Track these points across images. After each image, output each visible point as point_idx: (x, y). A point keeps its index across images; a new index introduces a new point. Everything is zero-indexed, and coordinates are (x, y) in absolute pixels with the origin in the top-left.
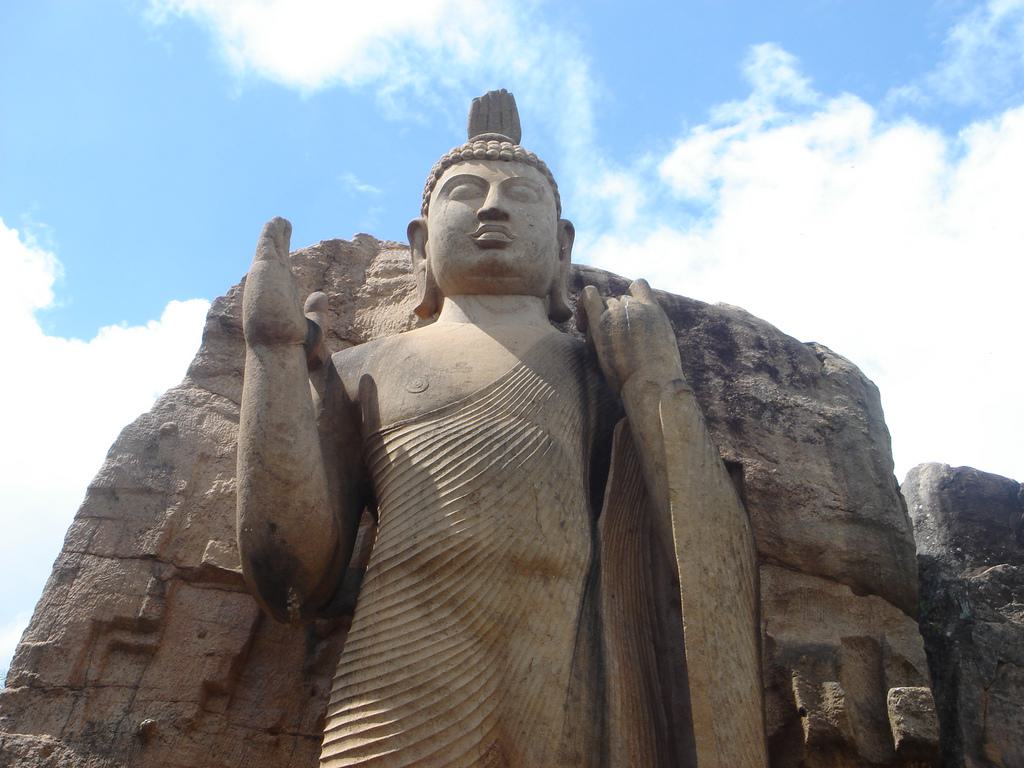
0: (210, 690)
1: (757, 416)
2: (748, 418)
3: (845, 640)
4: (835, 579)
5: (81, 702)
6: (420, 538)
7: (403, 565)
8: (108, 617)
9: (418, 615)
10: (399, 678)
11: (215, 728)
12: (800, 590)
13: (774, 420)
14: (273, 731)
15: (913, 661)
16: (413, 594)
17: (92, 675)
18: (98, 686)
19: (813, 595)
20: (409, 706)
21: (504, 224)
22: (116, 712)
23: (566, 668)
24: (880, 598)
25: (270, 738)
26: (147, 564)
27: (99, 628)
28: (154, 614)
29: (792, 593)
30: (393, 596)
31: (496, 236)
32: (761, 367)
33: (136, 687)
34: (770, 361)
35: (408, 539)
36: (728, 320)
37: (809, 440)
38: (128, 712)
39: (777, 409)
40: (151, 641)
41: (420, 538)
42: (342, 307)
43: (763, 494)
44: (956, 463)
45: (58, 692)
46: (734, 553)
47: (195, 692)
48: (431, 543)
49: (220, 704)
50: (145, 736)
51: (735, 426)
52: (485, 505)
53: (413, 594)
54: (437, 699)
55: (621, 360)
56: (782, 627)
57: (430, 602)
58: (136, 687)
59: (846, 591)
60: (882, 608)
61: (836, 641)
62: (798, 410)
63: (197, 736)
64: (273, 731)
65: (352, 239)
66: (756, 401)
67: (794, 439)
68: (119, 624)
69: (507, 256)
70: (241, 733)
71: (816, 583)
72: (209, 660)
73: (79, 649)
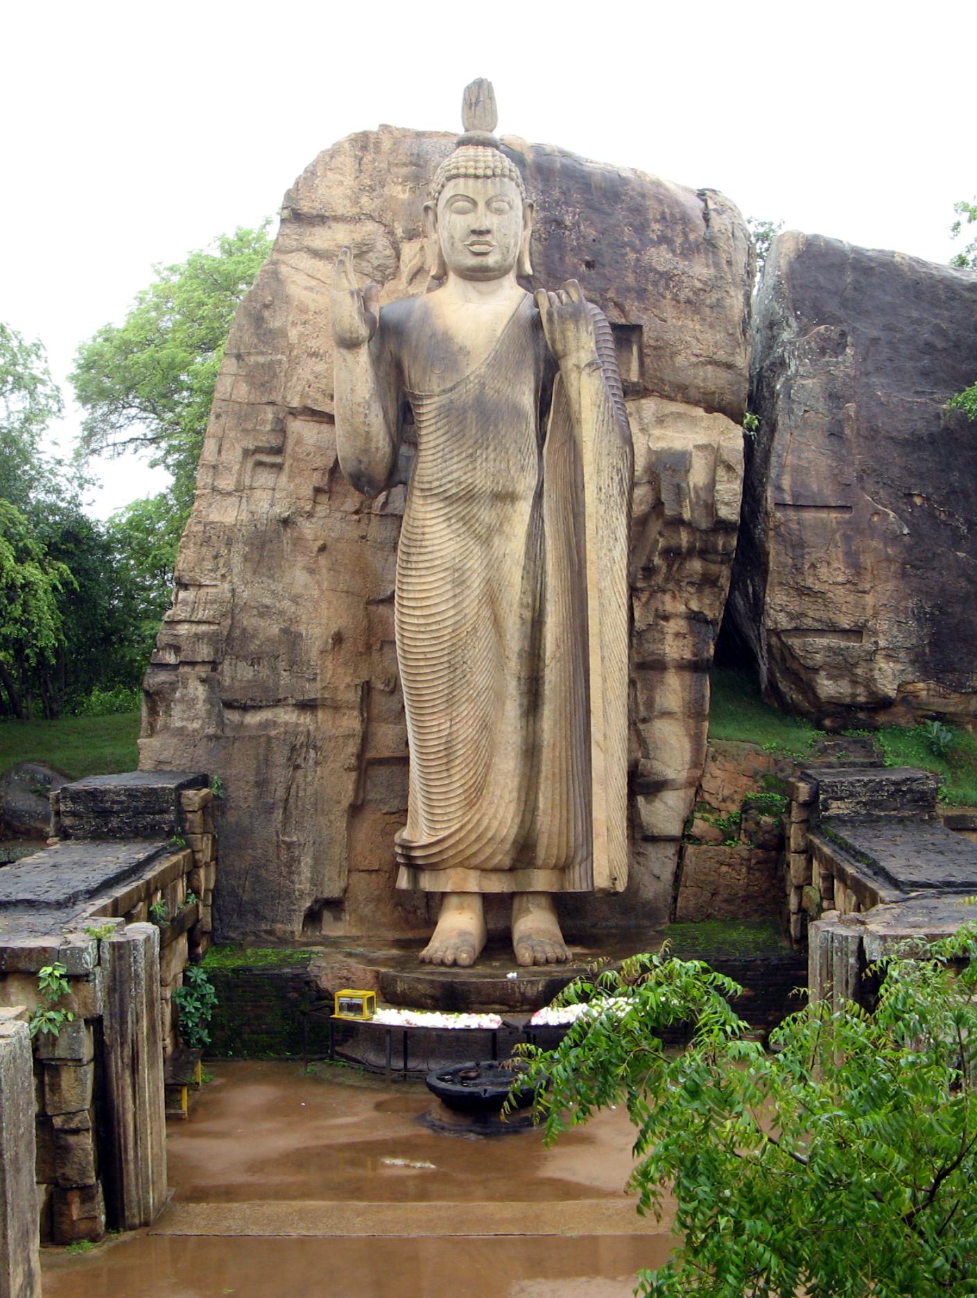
0: (318, 490)
1: (655, 284)
2: (650, 288)
3: (695, 447)
4: (696, 404)
5: (244, 500)
6: (444, 481)
8: (251, 447)
9: (444, 525)
11: (323, 514)
12: (672, 413)
13: (667, 287)
14: (356, 512)
15: (733, 462)
16: (441, 513)
17: (247, 482)
18: (251, 488)
19: (679, 416)
20: (442, 579)
21: (488, 238)
22: (265, 505)
23: (522, 557)
24: (721, 415)
25: (356, 517)
27: (246, 453)
29: (666, 415)
33: (274, 489)
34: (669, 233)
35: (437, 480)
36: (643, 196)
37: (689, 302)
39: (668, 277)
40: (278, 460)
41: (444, 481)
42: (374, 194)
43: (655, 348)
44: (809, 230)
45: (229, 494)
46: (619, 471)
48: (449, 486)
49: (323, 498)
51: (641, 294)
52: (479, 461)
53: (441, 513)
54: (457, 575)
56: (658, 438)
57: (449, 519)
58: (274, 489)
59: (700, 412)
60: (722, 420)
61: (690, 447)
62: (683, 278)
63: (314, 520)
64: (356, 512)
65: (375, 128)
66: (657, 272)
67: (678, 302)
68: (258, 450)
69: (491, 260)
70: (339, 515)
71: (680, 407)
73: (237, 467)
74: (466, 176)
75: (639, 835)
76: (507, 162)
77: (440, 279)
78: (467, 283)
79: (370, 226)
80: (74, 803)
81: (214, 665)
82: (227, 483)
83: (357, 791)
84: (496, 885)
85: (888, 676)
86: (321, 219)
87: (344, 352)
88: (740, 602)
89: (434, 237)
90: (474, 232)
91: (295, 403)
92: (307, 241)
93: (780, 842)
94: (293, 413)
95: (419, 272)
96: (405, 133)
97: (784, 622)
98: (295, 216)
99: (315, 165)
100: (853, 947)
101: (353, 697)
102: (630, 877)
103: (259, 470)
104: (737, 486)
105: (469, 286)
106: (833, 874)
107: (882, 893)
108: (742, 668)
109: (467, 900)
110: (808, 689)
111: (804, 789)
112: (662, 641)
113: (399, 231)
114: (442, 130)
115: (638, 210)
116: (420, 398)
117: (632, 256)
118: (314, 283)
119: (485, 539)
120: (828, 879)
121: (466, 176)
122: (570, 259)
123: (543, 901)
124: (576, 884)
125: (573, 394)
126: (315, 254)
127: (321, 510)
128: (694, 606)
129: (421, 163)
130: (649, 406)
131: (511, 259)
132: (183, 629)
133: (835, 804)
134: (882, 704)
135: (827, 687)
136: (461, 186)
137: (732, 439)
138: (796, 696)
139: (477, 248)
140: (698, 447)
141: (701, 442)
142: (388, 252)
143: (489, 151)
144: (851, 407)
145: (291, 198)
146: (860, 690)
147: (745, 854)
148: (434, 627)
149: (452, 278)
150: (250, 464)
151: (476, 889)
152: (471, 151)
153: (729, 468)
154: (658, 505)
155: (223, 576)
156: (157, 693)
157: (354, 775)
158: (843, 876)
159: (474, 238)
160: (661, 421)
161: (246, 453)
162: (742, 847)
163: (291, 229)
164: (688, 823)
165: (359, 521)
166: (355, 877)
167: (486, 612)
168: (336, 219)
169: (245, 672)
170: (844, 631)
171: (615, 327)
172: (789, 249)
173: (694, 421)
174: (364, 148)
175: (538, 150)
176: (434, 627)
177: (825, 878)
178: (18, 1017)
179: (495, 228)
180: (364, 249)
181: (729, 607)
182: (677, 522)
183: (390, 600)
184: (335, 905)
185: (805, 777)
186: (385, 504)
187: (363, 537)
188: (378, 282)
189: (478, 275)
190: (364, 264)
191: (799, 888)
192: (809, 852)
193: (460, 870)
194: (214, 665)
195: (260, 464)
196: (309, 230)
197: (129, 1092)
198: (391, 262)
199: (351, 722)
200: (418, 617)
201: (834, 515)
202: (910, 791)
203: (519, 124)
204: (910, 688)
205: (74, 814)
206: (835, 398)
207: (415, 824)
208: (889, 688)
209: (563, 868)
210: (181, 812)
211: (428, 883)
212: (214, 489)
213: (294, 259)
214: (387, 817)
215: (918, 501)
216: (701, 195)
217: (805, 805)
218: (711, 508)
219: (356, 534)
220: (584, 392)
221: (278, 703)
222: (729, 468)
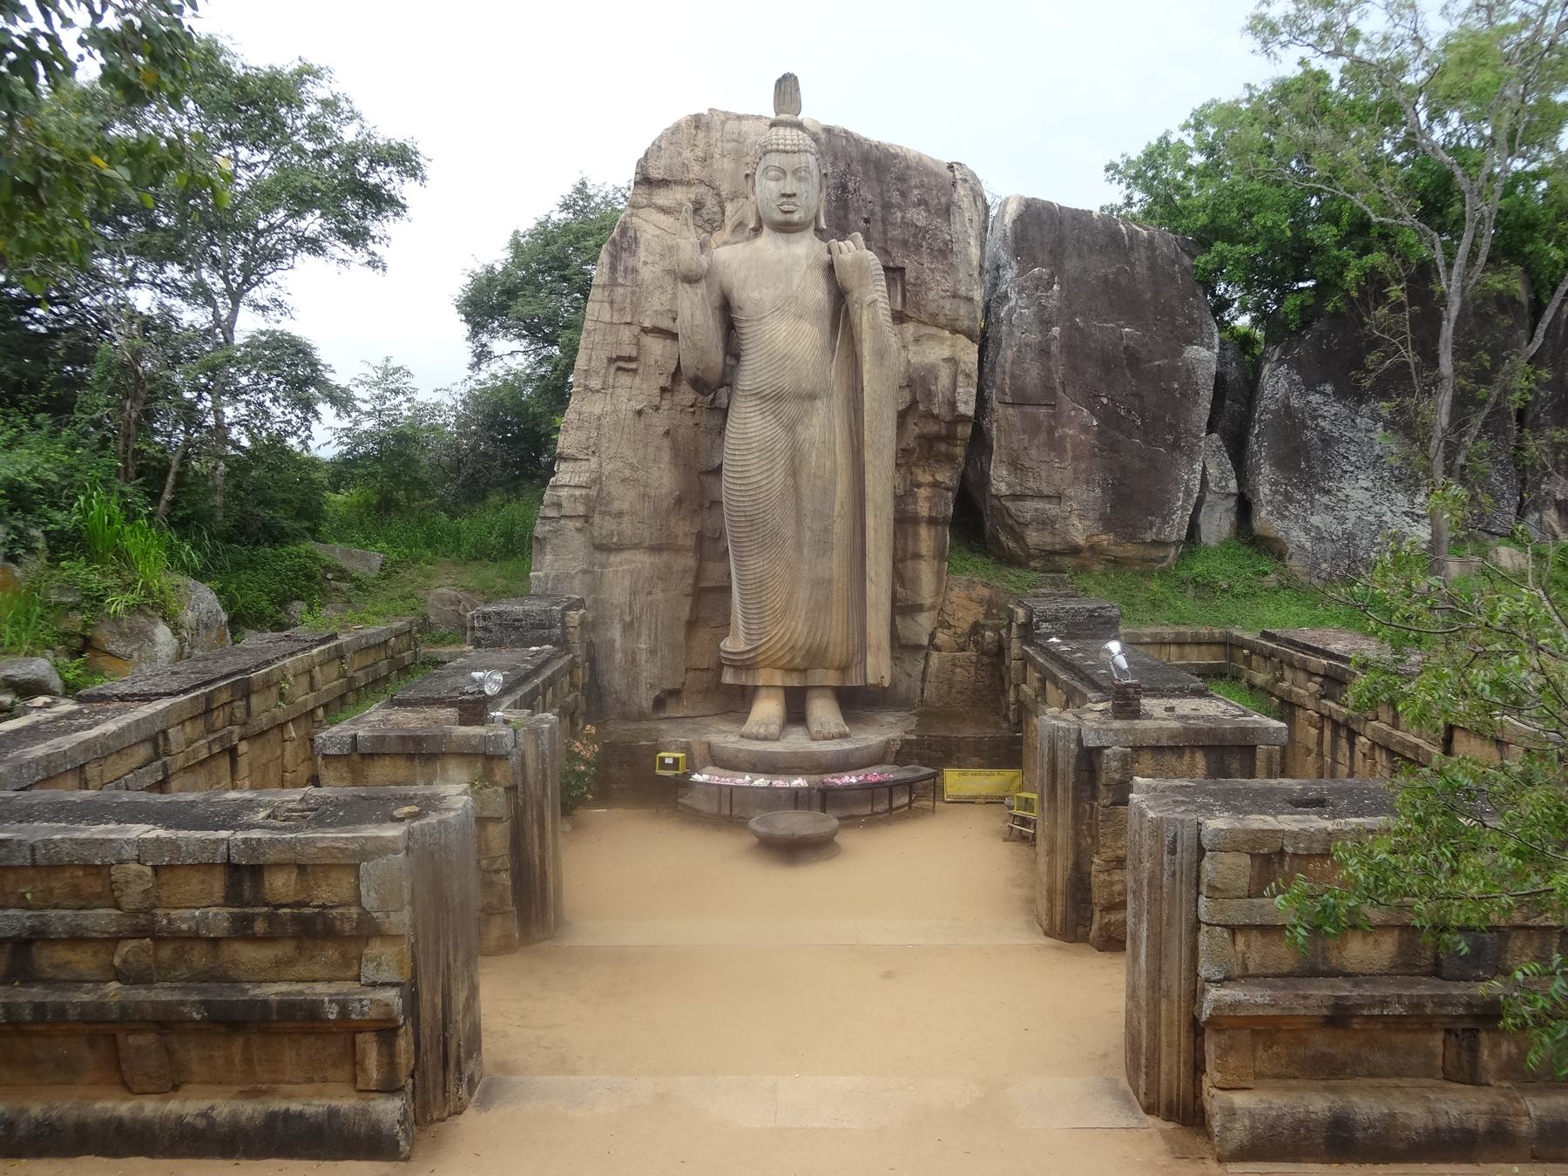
0: (663, 390)
19: (931, 337)
27: (611, 360)
28: (634, 354)
31: (791, 208)
32: (920, 203)
36: (908, 167)
40: (633, 366)
44: (1029, 195)
47: (657, 392)
49: (667, 395)
50: (640, 413)
60: (962, 340)
65: (706, 112)
68: (620, 358)
69: (795, 217)
71: (934, 330)
75: (900, 646)
76: (809, 141)
77: (757, 231)
79: (702, 189)
81: (586, 518)
82: (595, 383)
83: (692, 610)
84: (794, 681)
85: (1078, 532)
86: (664, 183)
87: (687, 286)
88: (971, 475)
89: (752, 198)
90: (784, 195)
91: (647, 324)
93: (1000, 650)
94: (645, 331)
95: (740, 225)
96: (728, 117)
97: (1003, 488)
98: (645, 181)
99: (660, 138)
100: (1074, 736)
101: (690, 542)
102: (892, 675)
104: (974, 391)
105: (780, 239)
106: (1046, 677)
107: (1090, 695)
108: (974, 524)
109: (772, 691)
110: (1020, 538)
111: (1021, 614)
112: (916, 502)
113: (724, 194)
115: (902, 179)
117: (899, 215)
118: (659, 232)
119: (791, 428)
120: (1043, 681)
122: (852, 217)
123: (829, 693)
124: (855, 680)
125: (857, 320)
126: (663, 210)
127: (666, 405)
128: (939, 477)
130: (910, 329)
131: (811, 216)
132: (564, 493)
133: (1045, 625)
134: (1075, 551)
135: (1033, 537)
136: (774, 160)
137: (969, 354)
138: (1012, 545)
139: (785, 208)
140: (944, 360)
141: (947, 356)
143: (795, 131)
144: (1056, 331)
145: (642, 166)
146: (1058, 539)
147: (974, 659)
149: (765, 229)
151: (779, 683)
152: (781, 131)
153: (968, 376)
154: (914, 403)
157: (690, 599)
158: (1055, 680)
160: (917, 340)
162: (971, 653)
163: (642, 190)
164: (932, 636)
166: (691, 675)
167: (790, 482)
168: (676, 182)
169: (610, 525)
170: (1048, 497)
171: (886, 269)
172: (1012, 210)
173: (942, 340)
174: (697, 127)
175: (828, 130)
177: (1039, 680)
178: (465, 793)
179: (798, 192)
181: (963, 479)
182: (930, 415)
183: (718, 471)
184: (675, 693)
185: (1020, 604)
186: (713, 400)
189: (786, 228)
191: (1017, 686)
192: (1026, 660)
193: (769, 670)
194: (586, 518)
195: (619, 369)
197: (536, 840)
198: (718, 217)
199: (690, 561)
201: (1043, 410)
202: (1101, 616)
203: (817, 110)
204: (1095, 539)
205: (485, 629)
206: (1046, 324)
207: (736, 636)
208: (1080, 540)
209: (844, 669)
210: (564, 626)
211: (744, 680)
212: (586, 388)
213: (644, 213)
215: (1105, 401)
216: (950, 167)
217: (1019, 626)
218: (952, 404)
219: (689, 421)
220: (865, 318)
222: (968, 376)
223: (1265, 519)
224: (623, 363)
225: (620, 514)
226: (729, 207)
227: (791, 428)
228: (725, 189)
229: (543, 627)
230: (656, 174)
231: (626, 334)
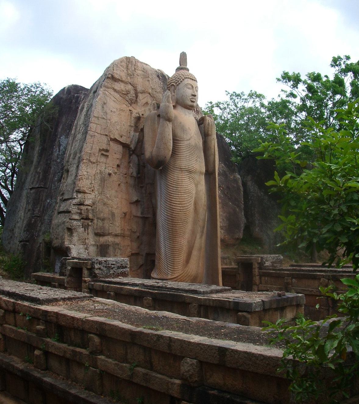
7: (186, 170)
8: (101, 148)
10: (187, 191)
26: (106, 136)
27: (100, 150)
30: (184, 175)
38: (105, 168)
45: (94, 163)
47: (116, 166)
48: (192, 168)
53: (188, 176)
55: (210, 133)
63: (117, 175)
65: (130, 56)
68: (103, 150)
72: (118, 160)
74: (191, 79)
78: (186, 110)
80: (100, 265)
82: (93, 159)
90: (193, 95)
92: (113, 86)
94: (112, 140)
103: (102, 156)
114: (146, 63)
116: (178, 140)
118: (115, 100)
121: (191, 79)
126: (115, 90)
129: (145, 71)
142: (134, 95)
148: (185, 210)
150: (100, 154)
155: (93, 190)
156: (75, 229)
159: (193, 97)
161: (100, 150)
165: (126, 177)
168: (122, 81)
169: (100, 223)
176: (185, 210)
180: (128, 92)
187: (127, 182)
188: (129, 104)
190: (127, 97)
195: (102, 154)
196: (116, 83)
198: (134, 98)
200: (180, 207)
212: (90, 161)
214: (133, 272)
221: (109, 234)
223: (257, 230)
224: (104, 153)
225: (103, 220)
226: (140, 96)
227: (196, 185)
228: (139, 88)
229: (123, 268)
230: (116, 76)
231: (105, 139)
